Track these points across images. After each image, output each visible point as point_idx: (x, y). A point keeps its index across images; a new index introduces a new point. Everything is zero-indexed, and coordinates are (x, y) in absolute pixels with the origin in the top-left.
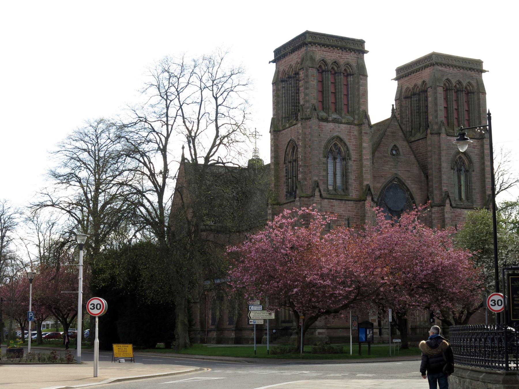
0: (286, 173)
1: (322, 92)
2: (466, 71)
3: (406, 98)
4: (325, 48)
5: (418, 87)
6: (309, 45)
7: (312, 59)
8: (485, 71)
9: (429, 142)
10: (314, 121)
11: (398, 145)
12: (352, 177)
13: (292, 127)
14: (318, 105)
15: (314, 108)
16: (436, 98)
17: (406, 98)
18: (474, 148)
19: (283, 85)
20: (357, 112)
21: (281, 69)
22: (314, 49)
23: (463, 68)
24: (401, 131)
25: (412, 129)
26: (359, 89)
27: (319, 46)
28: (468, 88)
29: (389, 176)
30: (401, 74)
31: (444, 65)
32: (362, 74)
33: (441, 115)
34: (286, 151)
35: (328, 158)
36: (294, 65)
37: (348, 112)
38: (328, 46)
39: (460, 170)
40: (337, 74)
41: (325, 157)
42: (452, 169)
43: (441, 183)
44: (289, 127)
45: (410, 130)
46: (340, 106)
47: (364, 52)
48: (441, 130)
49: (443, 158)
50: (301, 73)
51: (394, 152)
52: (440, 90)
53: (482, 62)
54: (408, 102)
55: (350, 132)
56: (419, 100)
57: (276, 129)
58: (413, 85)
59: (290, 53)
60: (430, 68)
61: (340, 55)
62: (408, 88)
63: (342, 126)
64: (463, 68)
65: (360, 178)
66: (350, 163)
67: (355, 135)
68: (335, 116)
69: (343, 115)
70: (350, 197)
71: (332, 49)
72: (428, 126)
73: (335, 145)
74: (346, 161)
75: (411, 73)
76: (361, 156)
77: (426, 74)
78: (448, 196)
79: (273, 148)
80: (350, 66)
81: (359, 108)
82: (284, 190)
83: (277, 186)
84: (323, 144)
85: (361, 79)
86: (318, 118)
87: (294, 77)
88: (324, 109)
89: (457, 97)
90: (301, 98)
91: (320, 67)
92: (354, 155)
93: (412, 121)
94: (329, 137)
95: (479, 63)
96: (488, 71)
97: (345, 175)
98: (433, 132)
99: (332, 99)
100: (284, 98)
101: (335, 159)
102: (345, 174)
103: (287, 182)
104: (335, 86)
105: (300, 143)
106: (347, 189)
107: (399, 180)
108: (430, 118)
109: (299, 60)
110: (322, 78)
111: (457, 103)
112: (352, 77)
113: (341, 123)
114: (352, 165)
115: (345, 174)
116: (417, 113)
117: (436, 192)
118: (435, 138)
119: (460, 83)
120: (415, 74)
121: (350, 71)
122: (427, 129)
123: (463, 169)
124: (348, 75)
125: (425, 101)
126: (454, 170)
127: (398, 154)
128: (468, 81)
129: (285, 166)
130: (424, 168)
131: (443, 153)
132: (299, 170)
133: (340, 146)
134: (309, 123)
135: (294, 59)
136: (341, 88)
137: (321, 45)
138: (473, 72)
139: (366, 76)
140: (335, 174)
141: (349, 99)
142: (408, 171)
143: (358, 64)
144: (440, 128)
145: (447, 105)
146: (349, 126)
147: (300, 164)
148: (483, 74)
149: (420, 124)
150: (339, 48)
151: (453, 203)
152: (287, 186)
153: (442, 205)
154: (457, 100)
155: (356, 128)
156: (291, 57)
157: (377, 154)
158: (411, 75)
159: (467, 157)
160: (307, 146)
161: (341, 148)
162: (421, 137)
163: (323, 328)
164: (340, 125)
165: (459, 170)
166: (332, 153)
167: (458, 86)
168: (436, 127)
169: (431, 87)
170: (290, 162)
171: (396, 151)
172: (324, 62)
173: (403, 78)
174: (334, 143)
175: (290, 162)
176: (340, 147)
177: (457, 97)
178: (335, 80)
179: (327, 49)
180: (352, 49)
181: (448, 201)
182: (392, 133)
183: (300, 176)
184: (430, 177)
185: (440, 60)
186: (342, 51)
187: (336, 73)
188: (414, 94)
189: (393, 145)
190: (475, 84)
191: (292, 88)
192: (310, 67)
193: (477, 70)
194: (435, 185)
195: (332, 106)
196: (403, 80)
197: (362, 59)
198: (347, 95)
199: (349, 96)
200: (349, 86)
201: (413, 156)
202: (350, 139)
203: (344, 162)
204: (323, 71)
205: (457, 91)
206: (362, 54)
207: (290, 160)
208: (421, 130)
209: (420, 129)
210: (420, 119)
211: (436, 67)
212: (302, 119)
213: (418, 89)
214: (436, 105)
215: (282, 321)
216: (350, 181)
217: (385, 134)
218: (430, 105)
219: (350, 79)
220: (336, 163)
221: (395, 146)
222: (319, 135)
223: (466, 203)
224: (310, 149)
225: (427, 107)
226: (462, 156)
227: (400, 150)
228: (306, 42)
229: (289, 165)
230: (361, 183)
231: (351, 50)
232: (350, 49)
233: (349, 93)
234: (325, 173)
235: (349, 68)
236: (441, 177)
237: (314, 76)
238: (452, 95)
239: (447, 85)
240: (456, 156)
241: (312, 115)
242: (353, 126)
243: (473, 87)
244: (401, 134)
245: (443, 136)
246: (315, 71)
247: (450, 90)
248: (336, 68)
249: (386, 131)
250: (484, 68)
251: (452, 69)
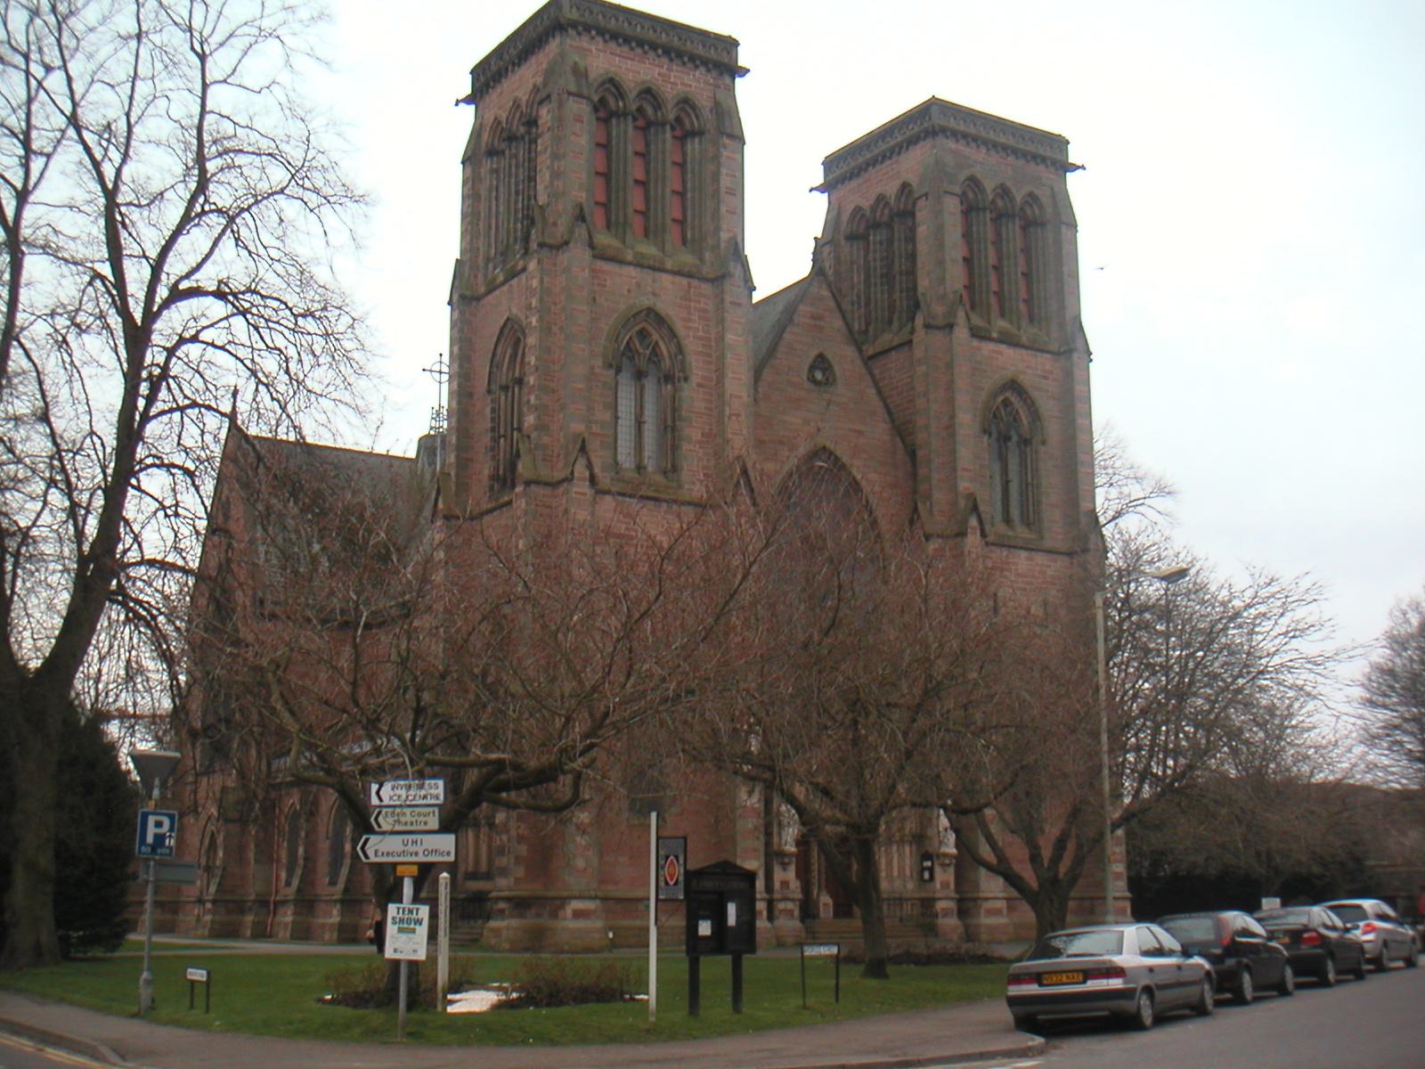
0: (493, 420)
1: (606, 176)
2: (1021, 162)
3: (851, 237)
4: (619, 45)
5: (887, 204)
6: (571, 32)
8: (1075, 168)
9: (919, 352)
10: (577, 257)
11: (829, 356)
12: (693, 432)
13: (514, 282)
14: (598, 217)
15: (578, 211)
16: (939, 231)
17: (851, 237)
18: (1046, 378)
20: (710, 241)
21: (489, 117)
22: (585, 45)
23: (1015, 152)
24: (838, 315)
25: (868, 324)
26: (716, 177)
27: (599, 39)
28: (1029, 212)
30: (838, 172)
31: (965, 136)
32: (728, 131)
33: (956, 277)
34: (494, 355)
35: (619, 370)
36: (524, 99)
37: (684, 242)
38: (627, 40)
39: (1008, 438)
40: (652, 130)
41: (611, 366)
42: (986, 432)
43: (954, 470)
44: (506, 281)
45: (863, 328)
46: (660, 222)
47: (737, 71)
48: (955, 315)
49: (962, 400)
50: (544, 112)
51: (819, 376)
52: (952, 205)
53: (1068, 143)
54: (858, 249)
55: (690, 300)
56: (890, 241)
57: (468, 293)
58: (873, 197)
59: (514, 64)
60: (922, 143)
61: (664, 71)
62: (858, 209)
63: (666, 279)
64: (1015, 152)
67: (705, 311)
69: (668, 247)
70: (684, 495)
71: (639, 51)
72: (917, 306)
73: (643, 334)
74: (673, 384)
75: (868, 165)
76: (720, 372)
77: (912, 164)
78: (975, 508)
79: (456, 349)
80: (694, 107)
81: (718, 229)
82: (483, 468)
84: (606, 326)
85: (725, 147)
86: (592, 246)
87: (523, 138)
89: (998, 233)
90: (540, 188)
91: (602, 101)
92: (698, 369)
93: (868, 303)
94: (622, 307)
95: (1060, 143)
96: (1083, 167)
97: (670, 428)
98: (932, 322)
99: (636, 199)
100: (494, 202)
101: (639, 375)
102: (669, 423)
103: (494, 449)
104: (647, 164)
105: (534, 320)
106: (675, 468)
108: (923, 283)
109: (539, 80)
110: (609, 135)
111: (999, 252)
112: (697, 140)
113: (662, 270)
114: (693, 397)
115: (669, 423)
116: (882, 276)
117: (938, 496)
118: (938, 337)
119: (1004, 191)
120: (878, 167)
121: (692, 124)
122: (913, 319)
123: (1015, 438)
124: (685, 135)
125: (906, 241)
126: (990, 435)
127: (830, 381)
128: (1027, 189)
129: (489, 399)
130: (903, 431)
131: (961, 383)
132: (529, 401)
133: (655, 336)
134: (564, 257)
136: (664, 170)
137: (607, 37)
138: (1042, 167)
139: (740, 139)
140: (639, 423)
141: (689, 203)
142: (860, 433)
143: (717, 104)
144: (951, 313)
145: (971, 250)
146: (685, 281)
147: (532, 382)
148: (1068, 174)
149: (892, 308)
150: (660, 51)
151: (988, 527)
152: (493, 458)
154: (998, 242)
155: (706, 288)
156: (517, 77)
157: (767, 374)
158: (866, 170)
159: (1025, 401)
160: (555, 328)
161: (661, 344)
162: (895, 343)
163: (591, 898)
164: (657, 275)
165: (1004, 439)
166: (632, 359)
167: (1000, 203)
168: (939, 309)
169: (926, 195)
170: (505, 388)
171: (824, 371)
172: (615, 86)
173: (843, 183)
174: (637, 328)
175: (505, 388)
176: (657, 343)
177: (998, 233)
178: (647, 145)
179: (626, 49)
180: (700, 58)
181: (973, 522)
182: (813, 317)
183: (530, 420)
184: (920, 453)
185: (952, 124)
186: (671, 60)
187: (649, 124)
188: (876, 225)
189: (814, 353)
190: (1045, 200)
191: (517, 167)
192: (570, 94)
193: (1054, 163)
194: (935, 476)
195: (637, 222)
196: (843, 190)
197: (731, 90)
198: (682, 195)
199: (689, 195)
200: (689, 166)
201: (873, 391)
202: (690, 320)
203: (669, 387)
204: (612, 114)
205: (1000, 217)
206: (727, 80)
207: (504, 382)
208: (896, 324)
209: (890, 322)
210: (890, 294)
211: (940, 140)
212: (541, 245)
213: (887, 212)
214: (940, 246)
215: (466, 873)
216: (685, 447)
217: (791, 320)
218: (923, 248)
219: (693, 146)
220: (642, 388)
221: (821, 356)
222: (594, 299)
223: (1022, 532)
224: (563, 337)
225: (912, 257)
226: (1012, 399)
227: (837, 369)
228: (562, 21)
229: (503, 398)
231: (698, 62)
232: (692, 58)
233: (689, 185)
234: (607, 416)
235: (689, 115)
236: (953, 452)
237: (582, 122)
238: (985, 224)
239: (971, 196)
240: (995, 396)
241: (571, 232)
242: (695, 282)
243: (1041, 207)
244: (838, 323)
245: (961, 333)
246: (584, 108)
247: (978, 210)
248: (650, 111)
249: (793, 313)
250: (1073, 157)
251: (984, 151)
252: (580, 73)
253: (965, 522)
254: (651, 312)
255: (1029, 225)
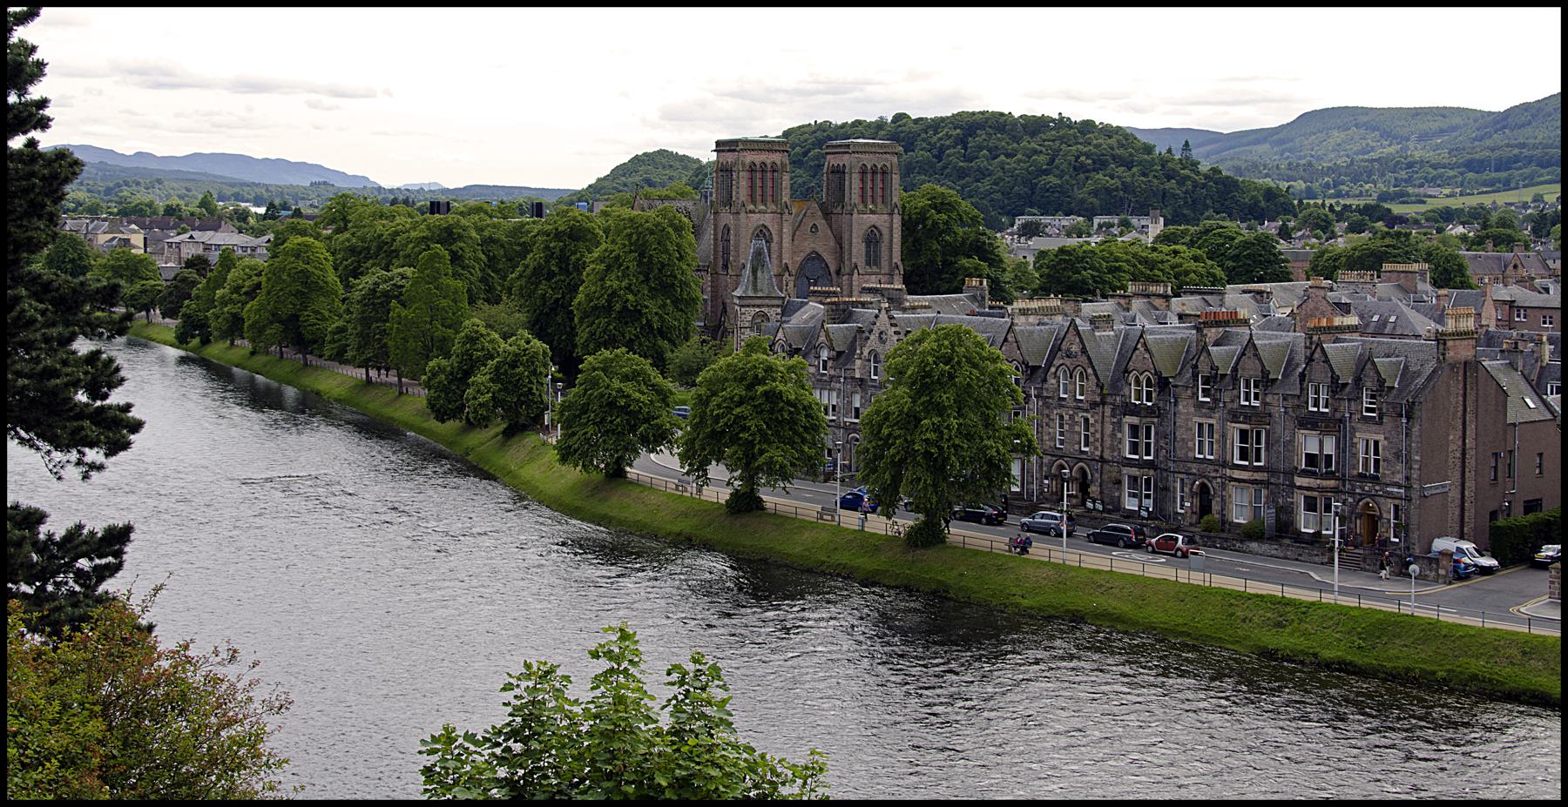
3: (832, 172)
7: (743, 164)
17: (832, 172)
19: (720, 174)
29: (808, 251)
52: (856, 178)
65: (780, 257)
66: (773, 245)
68: (763, 207)
73: (761, 231)
83: (715, 259)
84: (751, 231)
88: (753, 202)
92: (775, 238)
107: (817, 253)
114: (774, 246)
124: (774, 171)
130: (839, 240)
135: (730, 158)
144: (853, 210)
153: (851, 274)
168: (849, 208)
190: (889, 166)
205: (874, 172)
219: (775, 174)
230: (781, 262)
245: (855, 216)
252: (743, 164)
253: (853, 272)
254: (763, 225)
255: (884, 173)
